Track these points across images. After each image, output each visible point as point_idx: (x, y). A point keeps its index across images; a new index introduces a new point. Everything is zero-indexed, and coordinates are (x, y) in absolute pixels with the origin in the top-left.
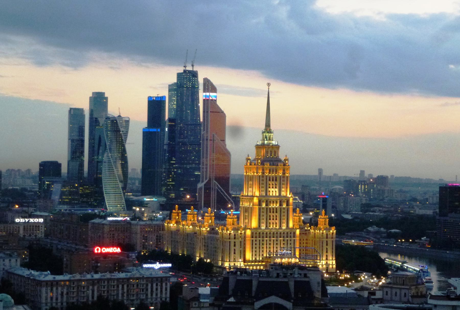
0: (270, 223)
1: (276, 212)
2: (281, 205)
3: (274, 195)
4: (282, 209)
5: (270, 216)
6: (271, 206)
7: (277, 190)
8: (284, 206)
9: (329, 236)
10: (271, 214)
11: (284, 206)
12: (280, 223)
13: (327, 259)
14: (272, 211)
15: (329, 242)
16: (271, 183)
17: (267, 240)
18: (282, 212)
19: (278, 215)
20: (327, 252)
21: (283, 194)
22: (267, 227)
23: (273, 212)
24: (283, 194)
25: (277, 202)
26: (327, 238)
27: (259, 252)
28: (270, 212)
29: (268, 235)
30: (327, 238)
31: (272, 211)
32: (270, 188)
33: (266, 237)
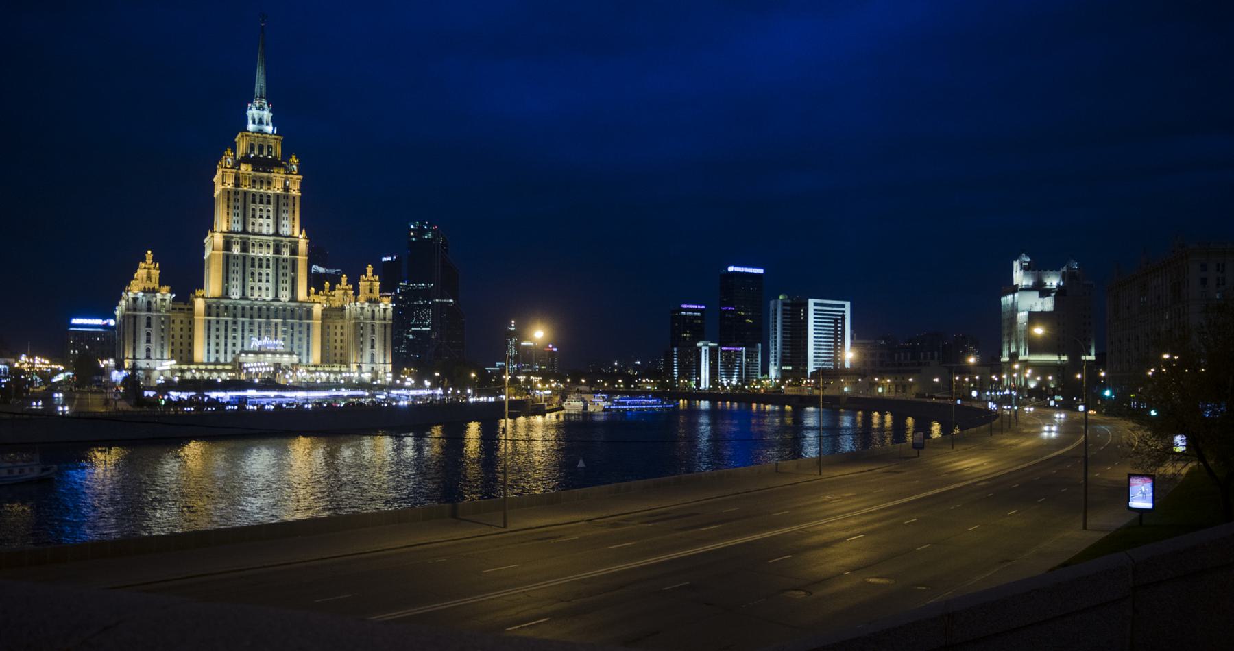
0: (252, 288)
1: (268, 266)
2: (277, 251)
5: (253, 274)
6: (255, 252)
7: (271, 221)
8: (286, 254)
9: (377, 314)
10: (257, 270)
11: (286, 254)
12: (277, 289)
13: (372, 361)
15: (377, 328)
19: (270, 271)
20: (373, 347)
22: (244, 294)
23: (260, 266)
24: (285, 230)
25: (268, 246)
28: (253, 266)
29: (248, 313)
30: (373, 318)
33: (243, 316)
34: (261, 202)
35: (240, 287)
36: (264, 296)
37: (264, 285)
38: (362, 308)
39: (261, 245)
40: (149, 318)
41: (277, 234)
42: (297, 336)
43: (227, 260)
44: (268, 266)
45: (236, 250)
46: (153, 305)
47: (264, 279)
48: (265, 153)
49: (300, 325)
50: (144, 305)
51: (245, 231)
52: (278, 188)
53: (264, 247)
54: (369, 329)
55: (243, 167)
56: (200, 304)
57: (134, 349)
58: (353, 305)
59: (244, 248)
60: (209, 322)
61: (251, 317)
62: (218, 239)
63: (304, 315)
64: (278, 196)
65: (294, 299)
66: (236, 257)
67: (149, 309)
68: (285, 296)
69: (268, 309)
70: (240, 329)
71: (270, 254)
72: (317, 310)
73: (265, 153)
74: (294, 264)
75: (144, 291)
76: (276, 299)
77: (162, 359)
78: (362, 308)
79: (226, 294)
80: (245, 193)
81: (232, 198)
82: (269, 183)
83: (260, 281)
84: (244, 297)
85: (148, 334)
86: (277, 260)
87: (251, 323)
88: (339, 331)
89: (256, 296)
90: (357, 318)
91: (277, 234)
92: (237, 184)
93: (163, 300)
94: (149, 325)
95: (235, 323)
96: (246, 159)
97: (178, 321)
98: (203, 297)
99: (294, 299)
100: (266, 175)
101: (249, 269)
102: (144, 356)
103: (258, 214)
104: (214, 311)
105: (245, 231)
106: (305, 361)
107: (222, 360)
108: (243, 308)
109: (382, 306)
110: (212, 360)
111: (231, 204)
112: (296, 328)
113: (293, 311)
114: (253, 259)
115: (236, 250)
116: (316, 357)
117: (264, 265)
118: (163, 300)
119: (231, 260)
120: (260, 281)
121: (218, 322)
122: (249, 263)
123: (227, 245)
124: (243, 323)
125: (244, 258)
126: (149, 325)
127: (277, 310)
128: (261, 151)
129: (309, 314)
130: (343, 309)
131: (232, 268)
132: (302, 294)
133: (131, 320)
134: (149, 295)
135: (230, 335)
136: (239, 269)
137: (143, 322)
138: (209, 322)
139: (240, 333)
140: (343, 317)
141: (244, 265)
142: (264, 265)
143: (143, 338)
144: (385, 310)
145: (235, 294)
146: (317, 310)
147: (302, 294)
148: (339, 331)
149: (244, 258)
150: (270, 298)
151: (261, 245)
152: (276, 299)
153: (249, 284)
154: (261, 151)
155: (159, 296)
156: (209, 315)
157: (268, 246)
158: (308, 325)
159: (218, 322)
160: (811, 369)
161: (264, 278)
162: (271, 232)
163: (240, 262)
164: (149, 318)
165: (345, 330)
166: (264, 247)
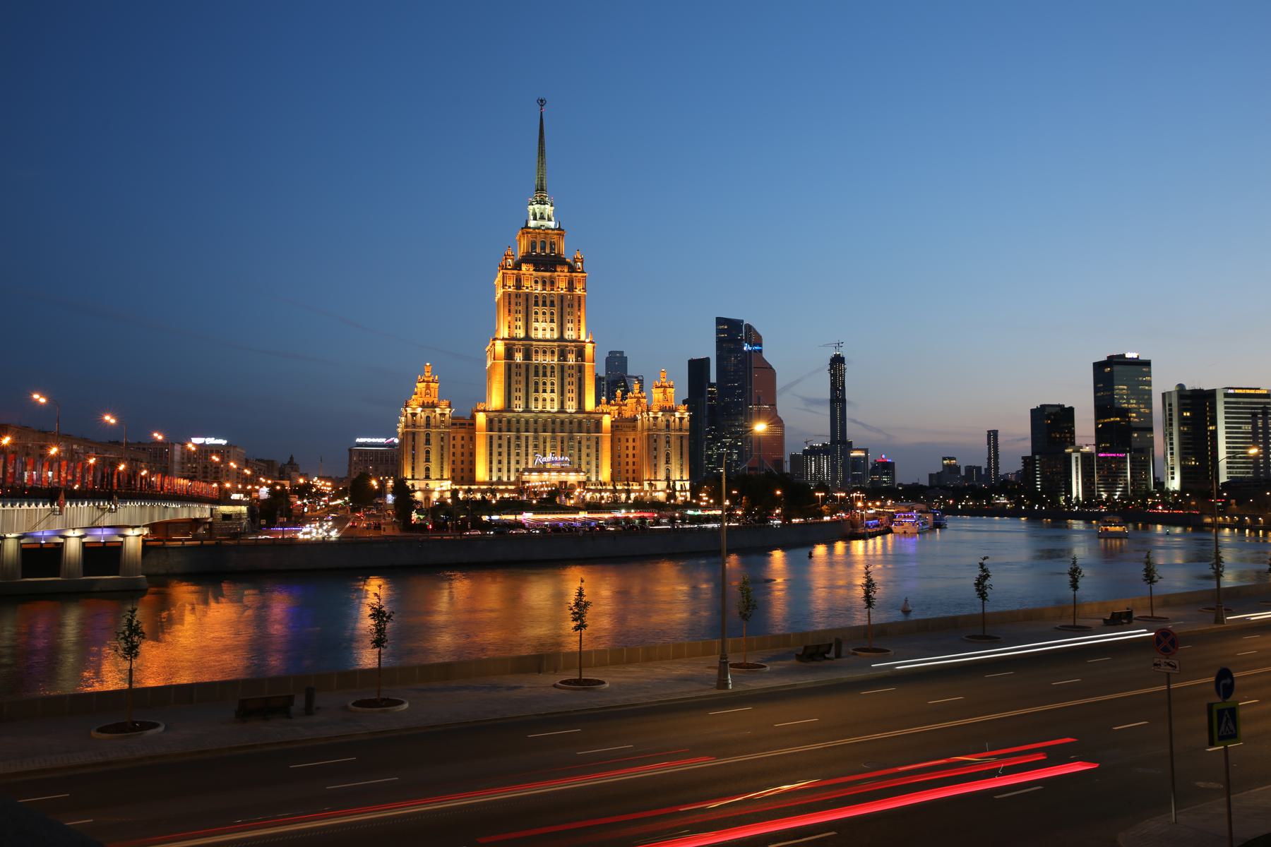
0: (536, 400)
2: (563, 355)
3: (548, 336)
5: (536, 383)
6: (540, 359)
7: (554, 325)
10: (541, 380)
14: (541, 373)
15: (672, 440)
16: (540, 309)
18: (566, 375)
19: (556, 380)
20: (667, 462)
21: (569, 334)
22: (527, 406)
23: (545, 375)
24: (569, 334)
25: (553, 352)
27: (509, 463)
29: (532, 426)
31: (541, 373)
32: (537, 321)
33: (527, 431)
34: (544, 304)
35: (523, 399)
36: (548, 409)
37: (548, 396)
38: (655, 418)
39: (545, 352)
40: (428, 435)
41: (561, 338)
42: (584, 451)
43: (509, 369)
45: (519, 357)
46: (432, 421)
47: (548, 390)
48: (548, 251)
49: (588, 439)
50: (423, 421)
51: (527, 337)
52: (562, 285)
53: (548, 353)
54: (663, 442)
55: (524, 267)
56: (481, 419)
57: (413, 469)
58: (645, 415)
59: (527, 356)
60: (491, 437)
62: (500, 347)
63: (592, 428)
64: (562, 297)
66: (519, 366)
68: (571, 407)
69: (554, 422)
70: (524, 444)
72: (607, 421)
73: (548, 251)
74: (581, 369)
75: (423, 406)
76: (562, 410)
77: (442, 479)
78: (655, 418)
79: (508, 407)
80: (527, 295)
81: (513, 301)
82: (552, 283)
83: (544, 391)
84: (527, 410)
85: (428, 452)
86: (562, 367)
87: (536, 438)
88: (630, 444)
89: (540, 408)
90: (649, 430)
91: (561, 338)
92: (518, 285)
93: (443, 415)
94: (428, 442)
95: (518, 438)
96: (527, 259)
97: (459, 437)
98: (484, 411)
100: (548, 274)
101: (533, 379)
102: (423, 476)
103: (540, 317)
105: (527, 337)
106: (593, 479)
107: (505, 479)
108: (527, 422)
109: (677, 415)
110: (495, 479)
111: (513, 308)
112: (584, 442)
114: (537, 367)
115: (519, 357)
116: (605, 474)
118: (443, 415)
119: (514, 369)
120: (544, 391)
121: (500, 438)
122: (532, 372)
123: (509, 354)
124: (527, 438)
125: (527, 367)
126: (428, 442)
127: (562, 422)
128: (543, 248)
129: (598, 426)
130: (635, 419)
131: (514, 378)
132: (590, 404)
133: (410, 437)
134: (428, 411)
135: (513, 452)
136: (522, 379)
137: (422, 438)
138: (491, 437)
139: (524, 448)
140: (635, 428)
143: (422, 457)
144: (681, 419)
145: (519, 405)
146: (607, 421)
147: (590, 404)
148: (630, 444)
149: (527, 367)
150: (556, 410)
151: (545, 352)
152: (562, 410)
153: (533, 395)
154: (543, 248)
155: (438, 411)
157: (553, 352)
159: (500, 438)
160: (1223, 478)
161: (549, 388)
163: (523, 371)
164: (428, 435)
165: (638, 443)
166: (548, 353)
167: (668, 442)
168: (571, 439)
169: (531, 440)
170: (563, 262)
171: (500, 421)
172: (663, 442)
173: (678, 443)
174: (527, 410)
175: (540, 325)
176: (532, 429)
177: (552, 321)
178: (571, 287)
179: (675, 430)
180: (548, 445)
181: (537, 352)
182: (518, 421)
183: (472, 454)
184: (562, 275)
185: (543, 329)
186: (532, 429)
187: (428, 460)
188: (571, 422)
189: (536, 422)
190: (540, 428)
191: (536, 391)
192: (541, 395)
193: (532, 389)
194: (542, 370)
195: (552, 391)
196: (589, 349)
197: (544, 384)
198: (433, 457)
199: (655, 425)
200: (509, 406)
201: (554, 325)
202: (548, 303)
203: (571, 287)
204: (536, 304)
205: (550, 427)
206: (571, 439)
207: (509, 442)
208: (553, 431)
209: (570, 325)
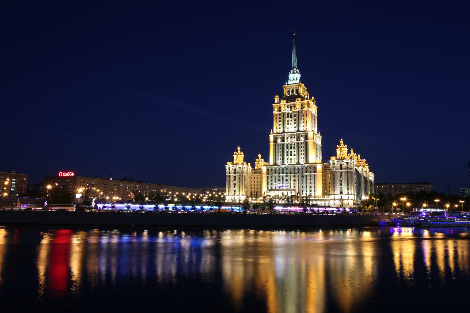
0: (288, 159)
3: (293, 131)
4: (300, 144)
5: (287, 152)
8: (302, 140)
9: (343, 166)
11: (302, 140)
14: (289, 147)
15: (343, 174)
17: (283, 177)
18: (300, 147)
22: (283, 162)
23: (291, 148)
24: (301, 129)
26: (341, 168)
28: (287, 148)
29: (285, 171)
30: (341, 168)
31: (289, 147)
32: (288, 124)
33: (283, 173)
34: (291, 117)
36: (293, 163)
39: (291, 138)
40: (235, 177)
41: (298, 131)
42: (309, 181)
44: (294, 148)
45: (279, 141)
49: (311, 176)
50: (233, 170)
51: (284, 132)
52: (298, 107)
53: (293, 138)
60: (268, 177)
61: (287, 173)
63: (312, 170)
65: (307, 162)
67: (235, 173)
68: (302, 161)
71: (293, 141)
74: (306, 144)
76: (298, 163)
79: (275, 164)
82: (295, 107)
83: (291, 155)
84: (283, 164)
91: (298, 131)
94: (235, 179)
99: (307, 162)
100: (292, 103)
101: (286, 150)
104: (270, 171)
105: (284, 132)
106: (313, 195)
109: (345, 161)
112: (308, 177)
113: (306, 168)
115: (279, 141)
117: (293, 147)
119: (277, 147)
120: (291, 155)
121: (272, 177)
126: (235, 179)
127: (298, 169)
129: (315, 170)
131: (278, 150)
136: (281, 150)
138: (268, 177)
141: (283, 148)
142: (293, 147)
145: (279, 162)
149: (283, 145)
151: (291, 138)
152: (298, 163)
153: (286, 158)
156: (268, 174)
157: (294, 137)
158: (314, 175)
161: (293, 153)
162: (296, 130)
164: (235, 177)
166: (293, 138)
167: (341, 175)
168: (302, 176)
169: (284, 177)
170: (299, 96)
171: (272, 170)
172: (338, 176)
173: (346, 174)
174: (283, 164)
175: (290, 126)
176: (293, 172)
177: (295, 123)
178: (302, 107)
179: (345, 169)
180: (292, 179)
181: (287, 138)
182: (279, 170)
183: (261, 185)
184: (298, 102)
185: (291, 127)
186: (285, 172)
187: (235, 187)
188: (302, 168)
189: (287, 169)
190: (289, 172)
191: (287, 155)
192: (290, 157)
193: (285, 154)
194: (289, 146)
195: (294, 155)
196: (310, 135)
197: (291, 152)
198: (237, 186)
199: (334, 167)
200: (276, 163)
201: (295, 125)
202: (293, 116)
203: (302, 107)
204: (288, 117)
205: (293, 171)
206: (302, 176)
207: (275, 179)
208: (295, 173)
209: (303, 124)
